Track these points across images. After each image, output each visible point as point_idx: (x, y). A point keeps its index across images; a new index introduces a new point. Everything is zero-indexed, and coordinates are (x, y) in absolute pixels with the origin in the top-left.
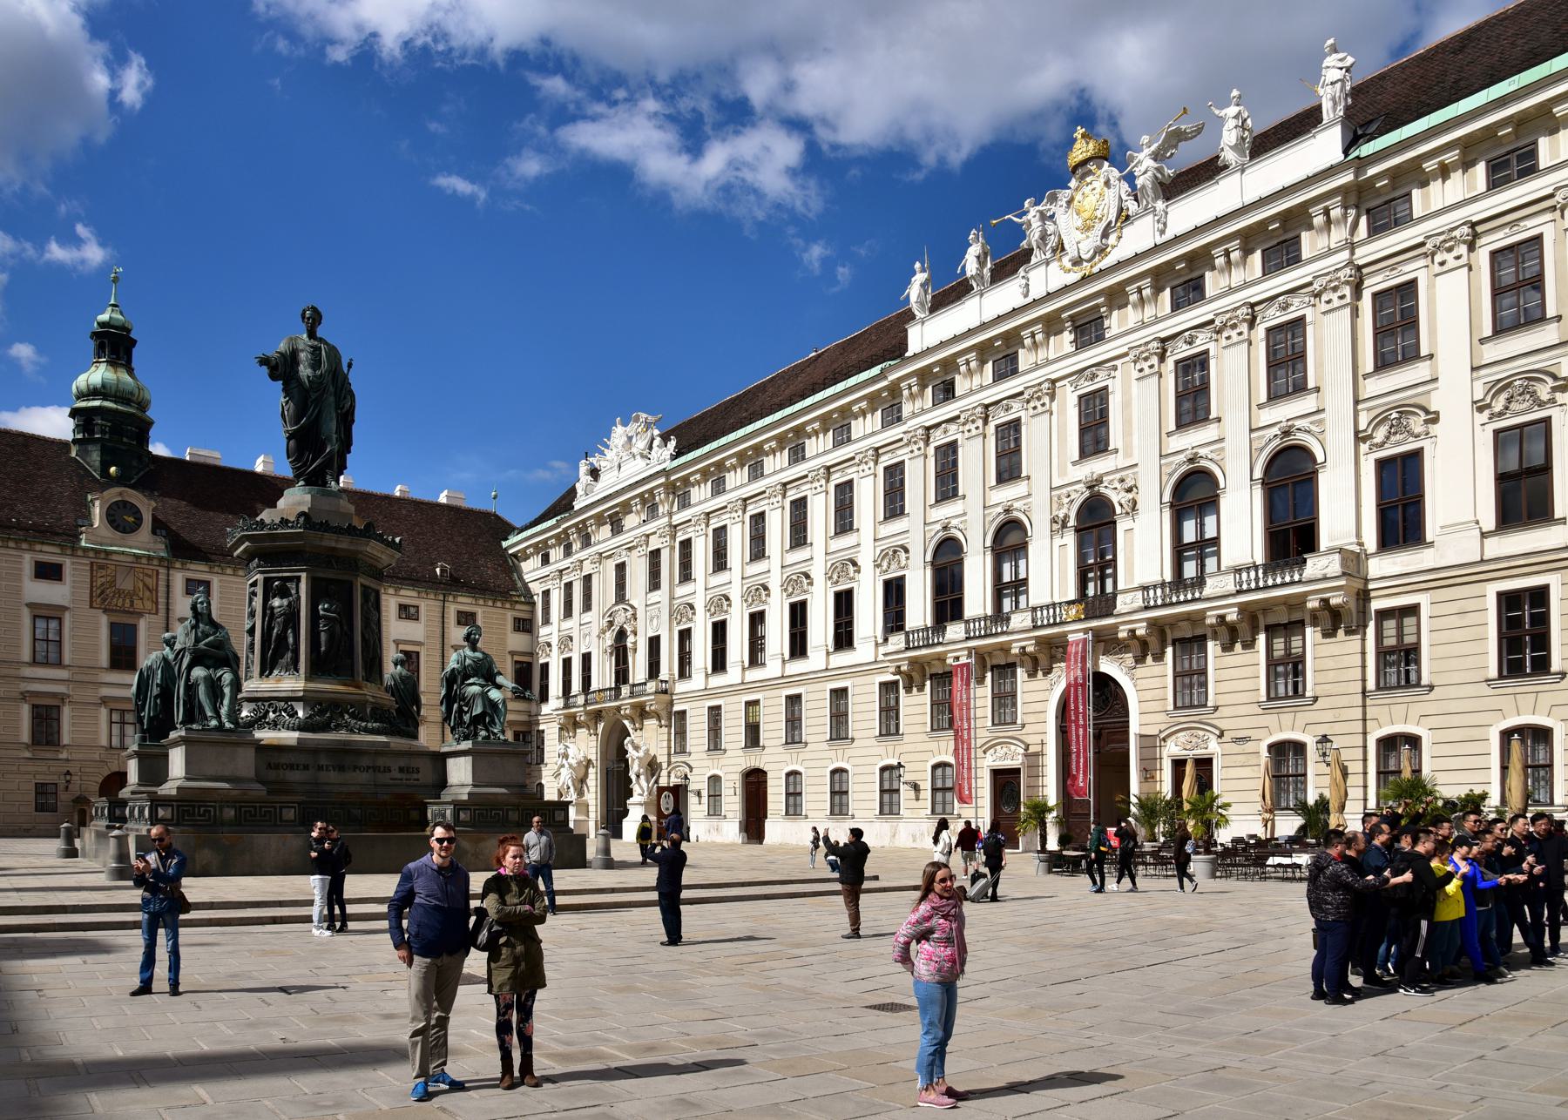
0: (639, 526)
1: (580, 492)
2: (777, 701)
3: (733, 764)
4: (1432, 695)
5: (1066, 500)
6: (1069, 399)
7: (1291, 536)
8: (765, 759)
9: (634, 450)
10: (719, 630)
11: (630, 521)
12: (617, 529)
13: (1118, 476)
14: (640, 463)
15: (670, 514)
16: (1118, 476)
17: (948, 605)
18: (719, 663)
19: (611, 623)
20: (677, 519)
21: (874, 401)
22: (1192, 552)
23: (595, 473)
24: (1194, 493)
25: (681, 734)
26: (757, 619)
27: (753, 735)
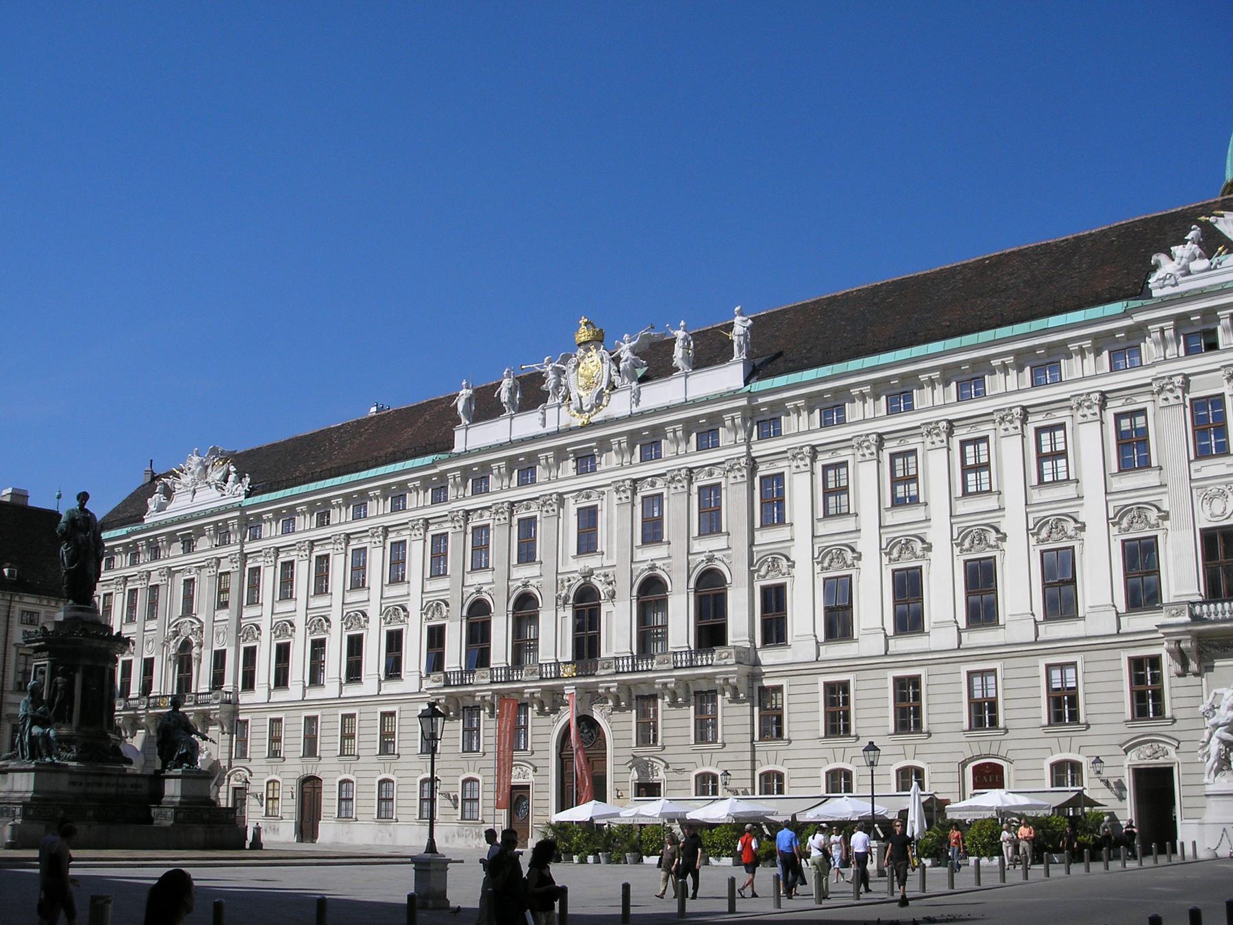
0: (212, 549)
1: (152, 507)
2: (332, 718)
3: (293, 768)
4: (790, 747)
5: (566, 584)
6: (572, 508)
7: (711, 634)
8: (320, 768)
9: (209, 479)
10: (283, 653)
11: (203, 543)
12: (189, 546)
13: (602, 571)
14: (216, 494)
15: (242, 543)
16: (602, 571)
17: (479, 654)
18: (281, 680)
19: (176, 634)
20: (250, 547)
21: (426, 483)
22: (649, 636)
23: (169, 493)
24: (651, 593)
25: (243, 742)
26: (318, 647)
27: (310, 748)
